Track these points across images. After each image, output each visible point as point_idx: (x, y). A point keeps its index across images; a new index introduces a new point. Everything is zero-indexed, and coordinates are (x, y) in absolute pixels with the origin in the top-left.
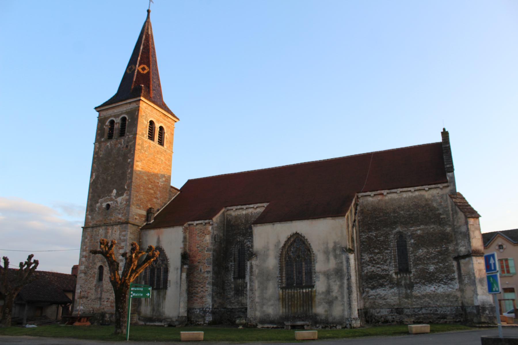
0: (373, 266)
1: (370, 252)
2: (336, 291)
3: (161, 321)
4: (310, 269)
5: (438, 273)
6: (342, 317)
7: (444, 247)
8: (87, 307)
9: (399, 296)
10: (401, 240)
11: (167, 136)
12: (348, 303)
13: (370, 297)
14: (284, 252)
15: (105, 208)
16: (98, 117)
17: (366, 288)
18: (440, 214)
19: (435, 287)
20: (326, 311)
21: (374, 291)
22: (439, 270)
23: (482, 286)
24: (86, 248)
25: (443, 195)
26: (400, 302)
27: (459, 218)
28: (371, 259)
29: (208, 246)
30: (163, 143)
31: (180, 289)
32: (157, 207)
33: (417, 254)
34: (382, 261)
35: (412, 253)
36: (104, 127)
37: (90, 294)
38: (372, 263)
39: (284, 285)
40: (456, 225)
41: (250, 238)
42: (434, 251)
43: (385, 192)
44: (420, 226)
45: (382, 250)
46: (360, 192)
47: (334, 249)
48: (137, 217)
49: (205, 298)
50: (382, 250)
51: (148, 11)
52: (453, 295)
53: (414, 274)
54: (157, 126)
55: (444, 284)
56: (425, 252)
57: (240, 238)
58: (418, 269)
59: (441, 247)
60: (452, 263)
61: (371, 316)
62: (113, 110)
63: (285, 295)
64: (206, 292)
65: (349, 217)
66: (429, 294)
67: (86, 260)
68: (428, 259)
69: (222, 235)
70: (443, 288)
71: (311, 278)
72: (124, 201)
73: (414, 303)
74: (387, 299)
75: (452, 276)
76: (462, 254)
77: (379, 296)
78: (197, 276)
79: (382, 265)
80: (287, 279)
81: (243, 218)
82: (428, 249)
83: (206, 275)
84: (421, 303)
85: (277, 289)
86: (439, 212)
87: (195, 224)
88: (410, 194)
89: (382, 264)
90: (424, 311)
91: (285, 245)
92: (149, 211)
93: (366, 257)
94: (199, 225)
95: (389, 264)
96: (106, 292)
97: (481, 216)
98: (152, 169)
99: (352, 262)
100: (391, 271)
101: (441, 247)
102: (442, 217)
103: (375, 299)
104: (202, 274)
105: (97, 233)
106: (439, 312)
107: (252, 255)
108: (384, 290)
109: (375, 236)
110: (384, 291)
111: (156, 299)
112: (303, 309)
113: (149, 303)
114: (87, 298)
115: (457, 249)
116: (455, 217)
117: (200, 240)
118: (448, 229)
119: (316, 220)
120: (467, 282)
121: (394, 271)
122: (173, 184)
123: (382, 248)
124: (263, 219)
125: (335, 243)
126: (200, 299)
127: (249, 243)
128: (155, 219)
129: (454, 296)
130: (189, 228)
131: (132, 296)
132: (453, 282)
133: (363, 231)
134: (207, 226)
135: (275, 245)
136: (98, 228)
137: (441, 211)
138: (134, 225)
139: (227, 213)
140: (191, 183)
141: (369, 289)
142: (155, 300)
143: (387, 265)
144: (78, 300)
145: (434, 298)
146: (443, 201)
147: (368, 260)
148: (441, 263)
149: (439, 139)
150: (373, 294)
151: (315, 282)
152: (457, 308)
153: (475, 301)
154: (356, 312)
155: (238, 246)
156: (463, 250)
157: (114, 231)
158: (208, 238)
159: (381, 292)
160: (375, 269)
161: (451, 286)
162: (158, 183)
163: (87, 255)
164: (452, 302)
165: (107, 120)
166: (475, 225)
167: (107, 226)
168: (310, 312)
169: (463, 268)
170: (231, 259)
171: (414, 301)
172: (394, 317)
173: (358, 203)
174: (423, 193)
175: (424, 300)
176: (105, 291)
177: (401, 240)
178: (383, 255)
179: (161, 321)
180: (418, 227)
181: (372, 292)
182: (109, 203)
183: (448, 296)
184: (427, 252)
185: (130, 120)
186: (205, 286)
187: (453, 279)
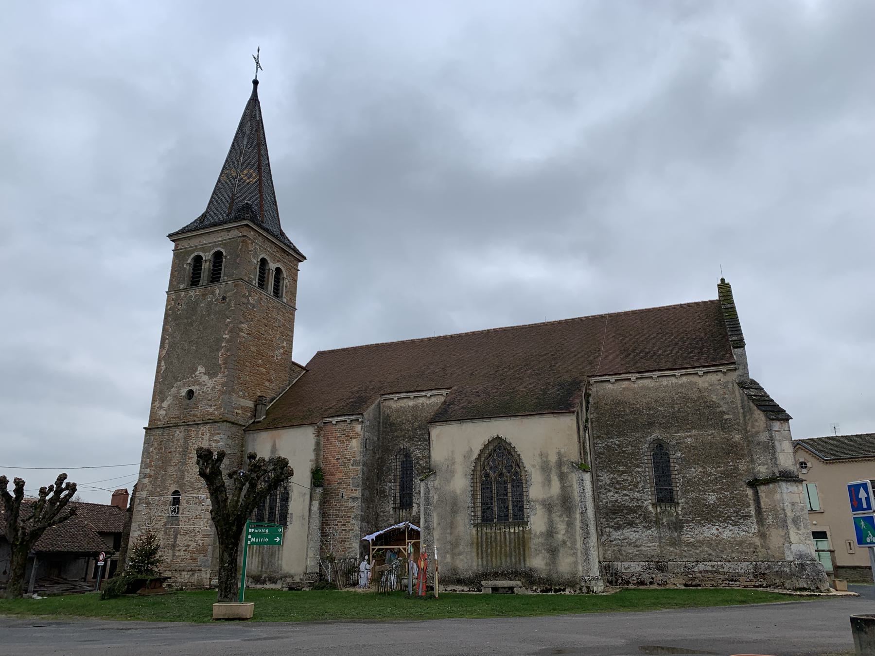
0: (617, 493)
1: (610, 470)
2: (563, 532)
3: (275, 583)
4: (521, 495)
5: (722, 507)
6: (574, 574)
7: (731, 465)
9: (660, 542)
10: (660, 451)
11: (286, 283)
12: (584, 551)
13: (614, 543)
14: (479, 467)
15: (185, 396)
16: (173, 250)
17: (605, 528)
19: (718, 529)
20: (547, 564)
21: (619, 533)
23: (798, 529)
26: (662, 552)
27: (756, 421)
28: (614, 480)
29: (355, 457)
30: (280, 294)
31: (309, 527)
32: (270, 395)
33: (687, 475)
34: (630, 485)
35: (679, 473)
36: (185, 266)
38: (615, 488)
39: (479, 521)
40: (749, 431)
41: (419, 443)
42: (715, 471)
43: (633, 377)
44: (690, 432)
45: (630, 467)
46: (593, 376)
47: (560, 464)
48: (240, 412)
49: (348, 542)
50: (630, 467)
51: (256, 83)
53: (682, 506)
54: (272, 266)
55: (733, 524)
56: (700, 472)
57: (404, 444)
58: (690, 498)
60: (746, 491)
61: (616, 574)
62: (200, 239)
63: (482, 538)
64: (351, 532)
65: (580, 415)
66: (708, 539)
68: (706, 483)
69: (376, 439)
70: (730, 530)
71: (521, 509)
72: (218, 386)
73: (684, 554)
74: (640, 547)
75: (746, 513)
77: (627, 541)
78: (335, 505)
79: (631, 492)
80: (484, 512)
81: (410, 412)
83: (350, 504)
85: (468, 527)
86: (718, 410)
88: (674, 380)
89: (631, 490)
90: (701, 567)
91: (479, 455)
92: (259, 401)
93: (605, 478)
94: (341, 423)
95: (642, 490)
96: (183, 535)
98: (264, 335)
99: (588, 485)
100: (645, 501)
102: (726, 417)
103: (622, 546)
104: (345, 502)
105: (171, 437)
106: (726, 570)
107: (429, 471)
108: (635, 531)
109: (619, 446)
110: (636, 533)
112: (511, 559)
113: (256, 553)
115: (753, 469)
116: (747, 418)
117: (341, 448)
118: (737, 437)
120: (771, 523)
121: (650, 501)
122: (294, 359)
123: (629, 465)
124: (443, 416)
125: (559, 454)
126: (341, 543)
128: (268, 413)
129: (750, 544)
130: (324, 429)
131: (249, 542)
133: (598, 437)
134: (354, 424)
135: (465, 456)
136: (173, 430)
137: (724, 408)
138: (233, 423)
139: (384, 404)
140: (321, 356)
141: (611, 530)
143: (638, 492)
145: (717, 546)
147: (608, 483)
149: (714, 295)
150: (617, 537)
151: (528, 517)
152: (756, 564)
153: (787, 553)
154: (597, 566)
155: (402, 457)
156: (763, 471)
157: (200, 434)
158: (355, 444)
159: (631, 534)
160: (620, 497)
162: (273, 357)
166: (783, 432)
168: (522, 565)
169: (764, 501)
170: (390, 477)
172: (654, 576)
173: (590, 392)
176: (182, 533)
177: (660, 451)
178: (632, 476)
179: (273, 581)
181: (616, 535)
182: (193, 388)
183: (740, 543)
185: (228, 257)
186: (350, 522)
187: (746, 517)
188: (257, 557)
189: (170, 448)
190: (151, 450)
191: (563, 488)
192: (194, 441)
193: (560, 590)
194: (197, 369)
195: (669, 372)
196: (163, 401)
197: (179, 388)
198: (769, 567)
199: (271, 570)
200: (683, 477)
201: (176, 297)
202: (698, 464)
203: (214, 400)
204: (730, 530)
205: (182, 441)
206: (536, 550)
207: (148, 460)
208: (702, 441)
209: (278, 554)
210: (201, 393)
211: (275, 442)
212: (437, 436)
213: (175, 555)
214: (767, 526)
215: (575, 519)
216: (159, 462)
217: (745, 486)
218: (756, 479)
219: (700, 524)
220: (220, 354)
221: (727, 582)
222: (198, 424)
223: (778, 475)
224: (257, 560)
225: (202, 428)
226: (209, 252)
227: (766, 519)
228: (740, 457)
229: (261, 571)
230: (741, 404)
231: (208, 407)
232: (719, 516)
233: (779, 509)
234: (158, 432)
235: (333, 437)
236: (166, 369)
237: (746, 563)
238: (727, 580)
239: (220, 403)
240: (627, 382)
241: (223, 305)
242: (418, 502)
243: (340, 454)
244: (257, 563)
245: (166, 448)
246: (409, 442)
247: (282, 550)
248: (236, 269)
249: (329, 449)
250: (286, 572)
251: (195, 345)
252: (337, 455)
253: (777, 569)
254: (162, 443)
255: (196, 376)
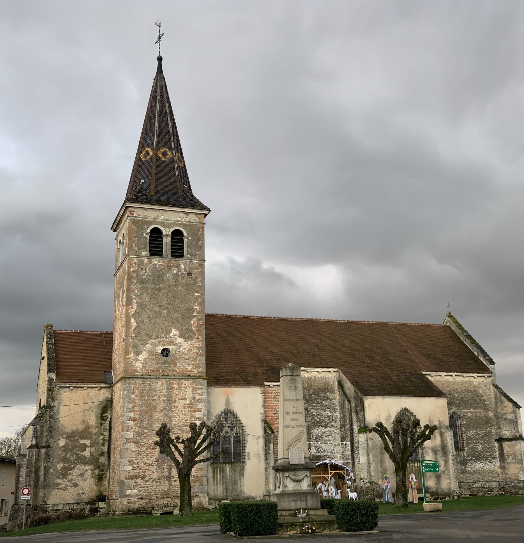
2: (443, 466)
7: (488, 430)
8: (144, 490)
18: (485, 400)
19: (482, 465)
20: (436, 484)
22: (485, 449)
24: (133, 407)
25: (486, 383)
27: (506, 407)
33: (469, 434)
35: (465, 433)
37: (147, 473)
40: (499, 412)
41: (314, 405)
43: (443, 374)
44: (470, 410)
52: (495, 471)
56: (475, 433)
59: (486, 430)
60: (494, 444)
66: (478, 470)
67: (136, 424)
70: (488, 465)
73: (468, 478)
75: (495, 456)
76: (505, 437)
81: (306, 381)
82: (476, 430)
84: (473, 477)
86: (483, 398)
87: (271, 386)
90: (476, 485)
97: (521, 407)
101: (486, 430)
102: (486, 403)
105: (153, 387)
106: (487, 486)
111: (229, 475)
113: (220, 482)
114: (144, 477)
115: (500, 432)
116: (499, 404)
117: (277, 405)
118: (491, 415)
119: (423, 398)
120: (511, 461)
125: (439, 421)
127: (313, 411)
129: (496, 472)
132: (495, 460)
135: (386, 419)
137: (485, 398)
142: (228, 476)
144: (126, 481)
145: (482, 474)
146: (486, 389)
148: (487, 444)
156: (507, 433)
157: (183, 387)
161: (494, 464)
163: (137, 417)
164: (495, 477)
165: (149, 226)
167: (169, 378)
171: (468, 477)
174: (472, 379)
175: (475, 475)
180: (468, 409)
182: (170, 347)
183: (492, 472)
184: (476, 433)
185: (190, 238)
187: (495, 458)
188: (222, 485)
189: (153, 397)
190: (133, 397)
191: (442, 441)
192: (177, 393)
193: (443, 498)
194: (170, 332)
195: (461, 374)
196: (138, 355)
197: (154, 345)
198: (507, 484)
199: (235, 494)
200: (467, 435)
201: (139, 261)
202: (474, 428)
203: (192, 360)
204: (488, 465)
205: (165, 392)
206: (430, 476)
207: (131, 405)
208: (475, 415)
209: (240, 482)
210: (178, 353)
211: (228, 396)
212: (369, 405)
213: (171, 485)
214: (507, 463)
215: (449, 458)
216: (144, 408)
217: (494, 441)
218: (501, 438)
219: (475, 461)
220: (192, 322)
221: (488, 493)
222: (180, 379)
223: (518, 437)
224: (222, 487)
225: (185, 382)
226: (170, 228)
227: (507, 459)
228: (492, 426)
229: (226, 496)
230: (494, 397)
231: (186, 365)
232: (483, 457)
233: (517, 454)
234: (138, 382)
235: (270, 397)
236: (137, 326)
237: (496, 482)
238: (488, 491)
239: (197, 363)
240: (439, 377)
241: (190, 280)
242: (315, 446)
243: (276, 410)
244: (222, 490)
245: (148, 396)
246: (307, 404)
247: (243, 479)
248: (199, 250)
249: (267, 405)
250: (248, 495)
251: (166, 310)
252: (274, 410)
253: (514, 485)
254: (144, 392)
255: (170, 337)
